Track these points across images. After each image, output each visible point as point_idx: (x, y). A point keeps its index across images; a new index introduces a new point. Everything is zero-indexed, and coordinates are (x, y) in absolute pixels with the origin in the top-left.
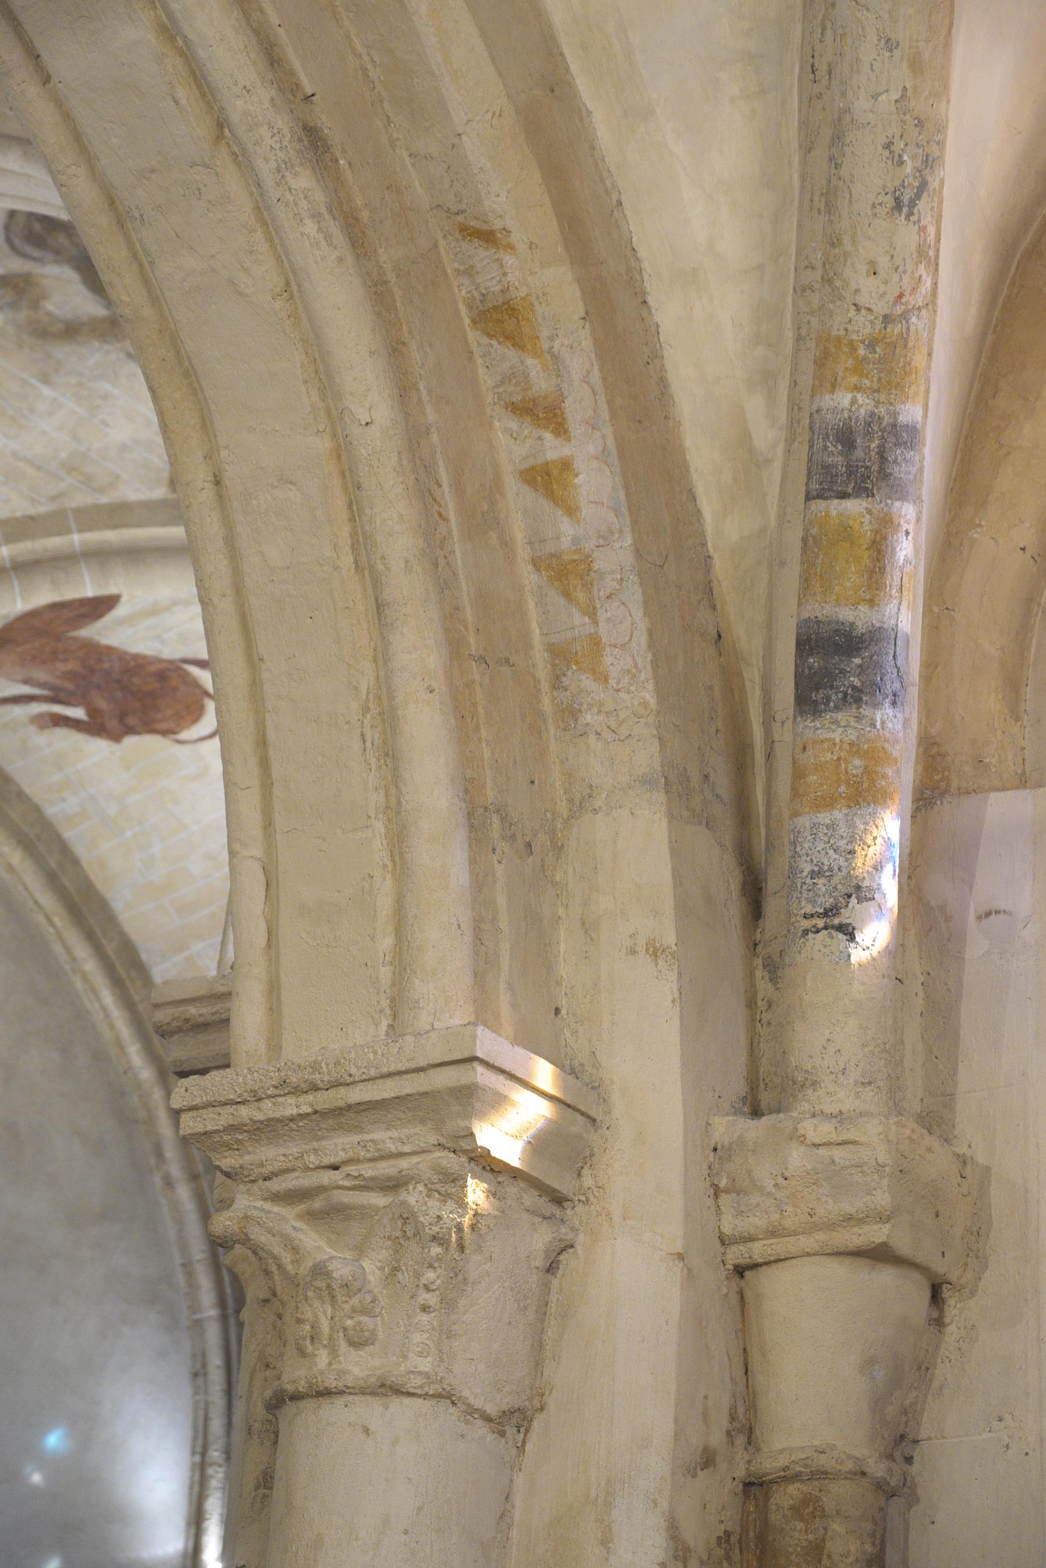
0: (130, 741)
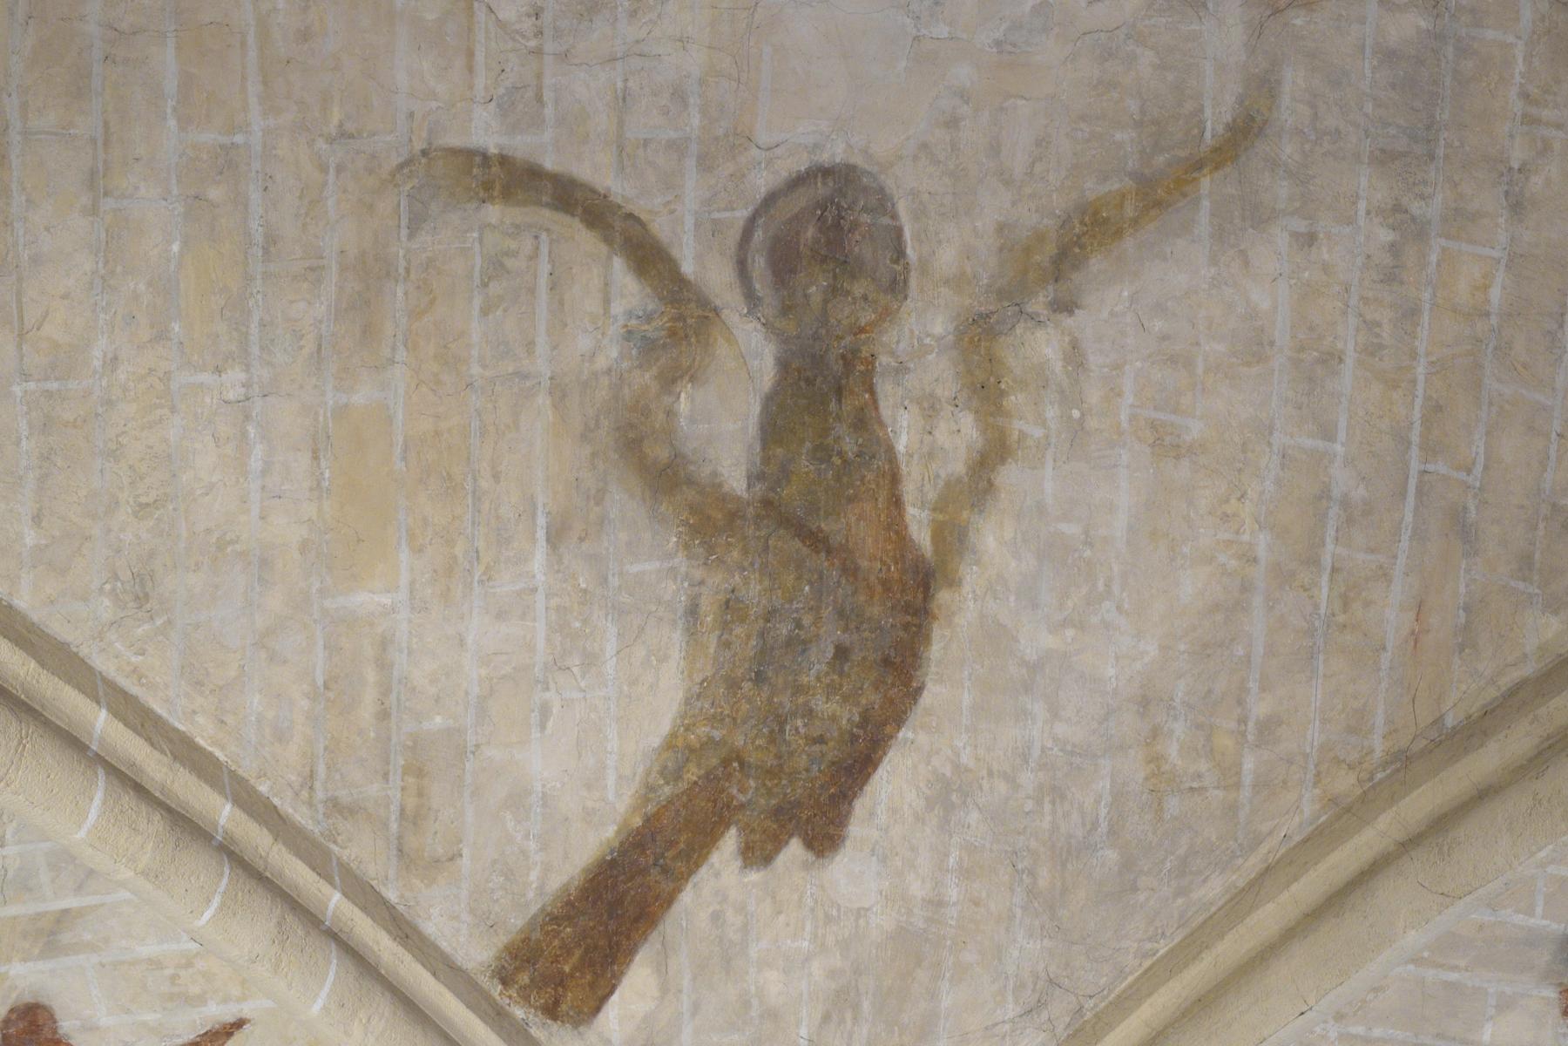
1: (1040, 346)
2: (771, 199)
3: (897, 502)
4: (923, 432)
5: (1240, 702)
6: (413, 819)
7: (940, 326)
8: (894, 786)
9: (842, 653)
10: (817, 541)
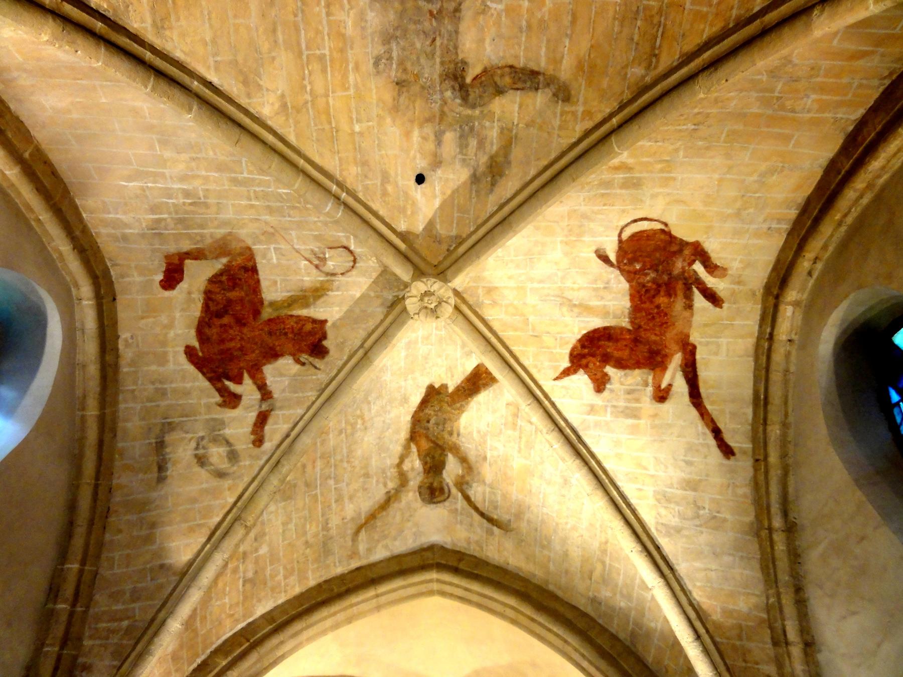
0: (690, 239)
1: (391, 485)
2: (445, 500)
3: (418, 451)
4: (414, 464)
5: (346, 436)
6: (516, 415)
7: (411, 483)
8: (416, 399)
9: (428, 422)
10: (433, 442)
